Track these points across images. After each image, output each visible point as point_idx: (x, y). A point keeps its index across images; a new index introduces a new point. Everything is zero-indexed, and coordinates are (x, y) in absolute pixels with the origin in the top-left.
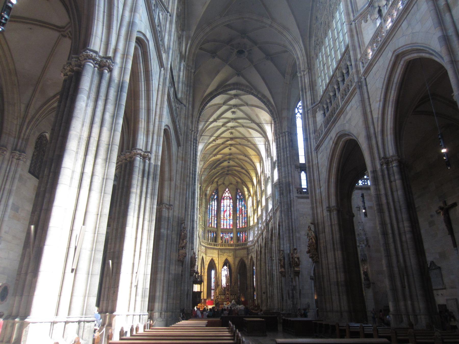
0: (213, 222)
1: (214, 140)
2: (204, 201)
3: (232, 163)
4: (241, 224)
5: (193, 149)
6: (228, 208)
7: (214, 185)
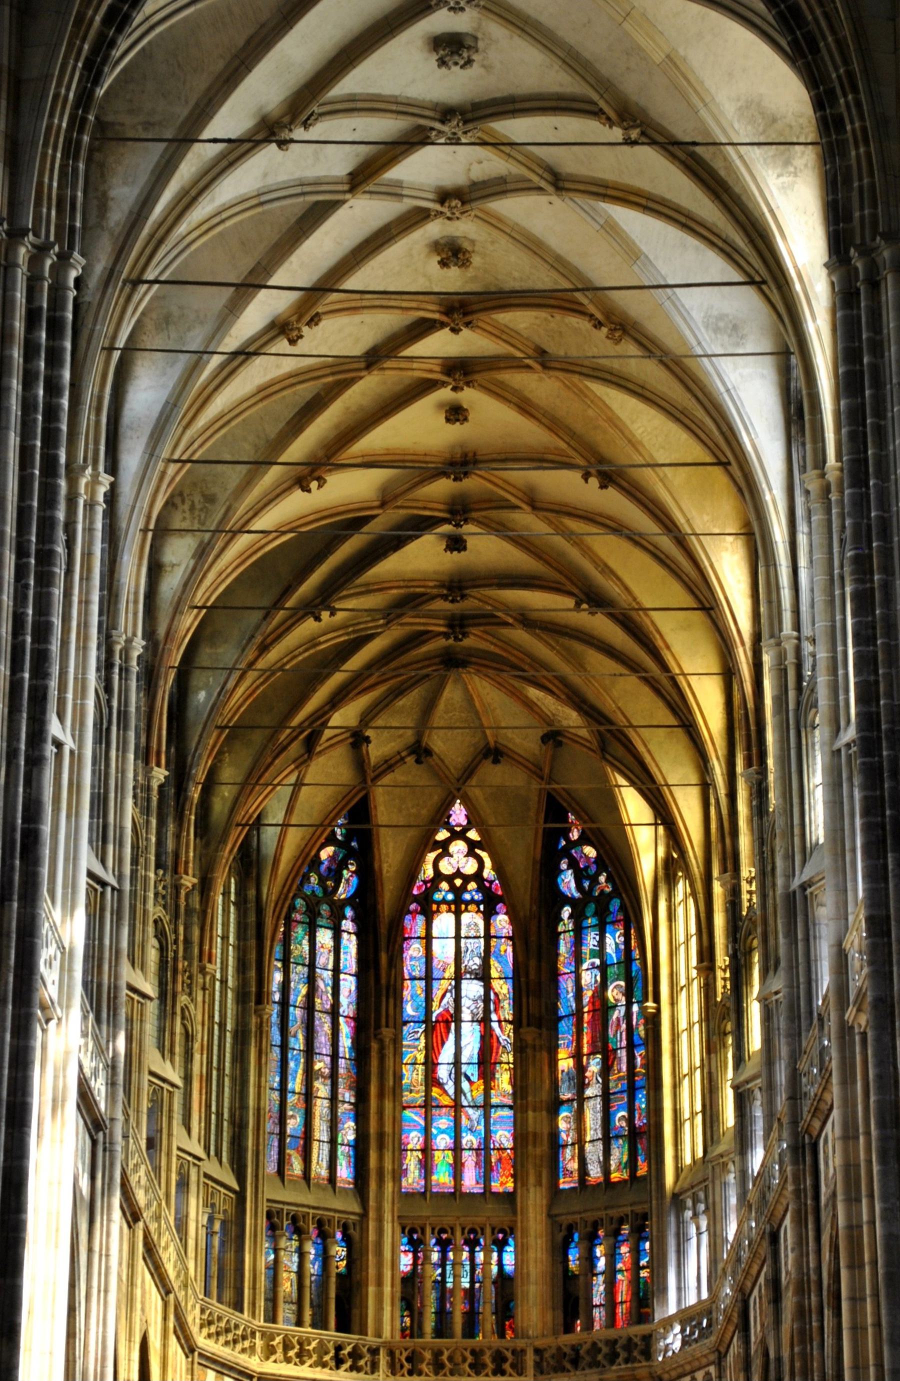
0: (321, 1131)
1: (282, 328)
2: (224, 919)
3: (485, 549)
4: (594, 1152)
5: (28, 406)
6: (472, 989)
7: (330, 770)
